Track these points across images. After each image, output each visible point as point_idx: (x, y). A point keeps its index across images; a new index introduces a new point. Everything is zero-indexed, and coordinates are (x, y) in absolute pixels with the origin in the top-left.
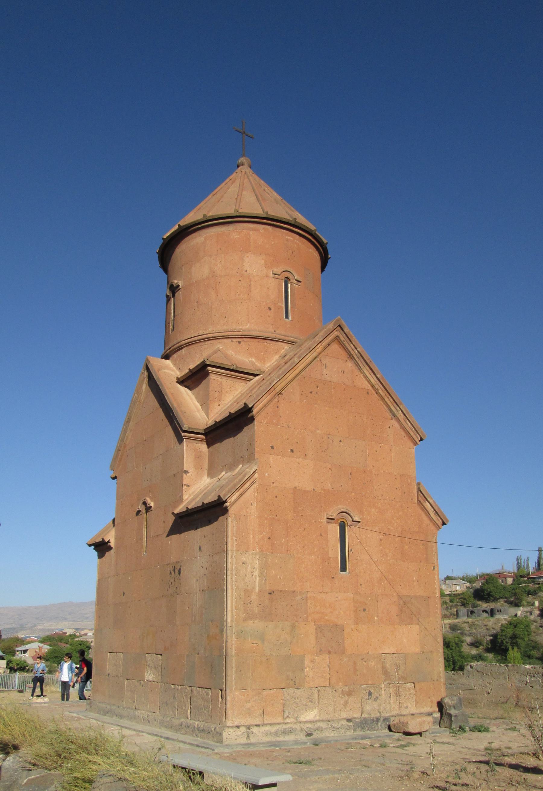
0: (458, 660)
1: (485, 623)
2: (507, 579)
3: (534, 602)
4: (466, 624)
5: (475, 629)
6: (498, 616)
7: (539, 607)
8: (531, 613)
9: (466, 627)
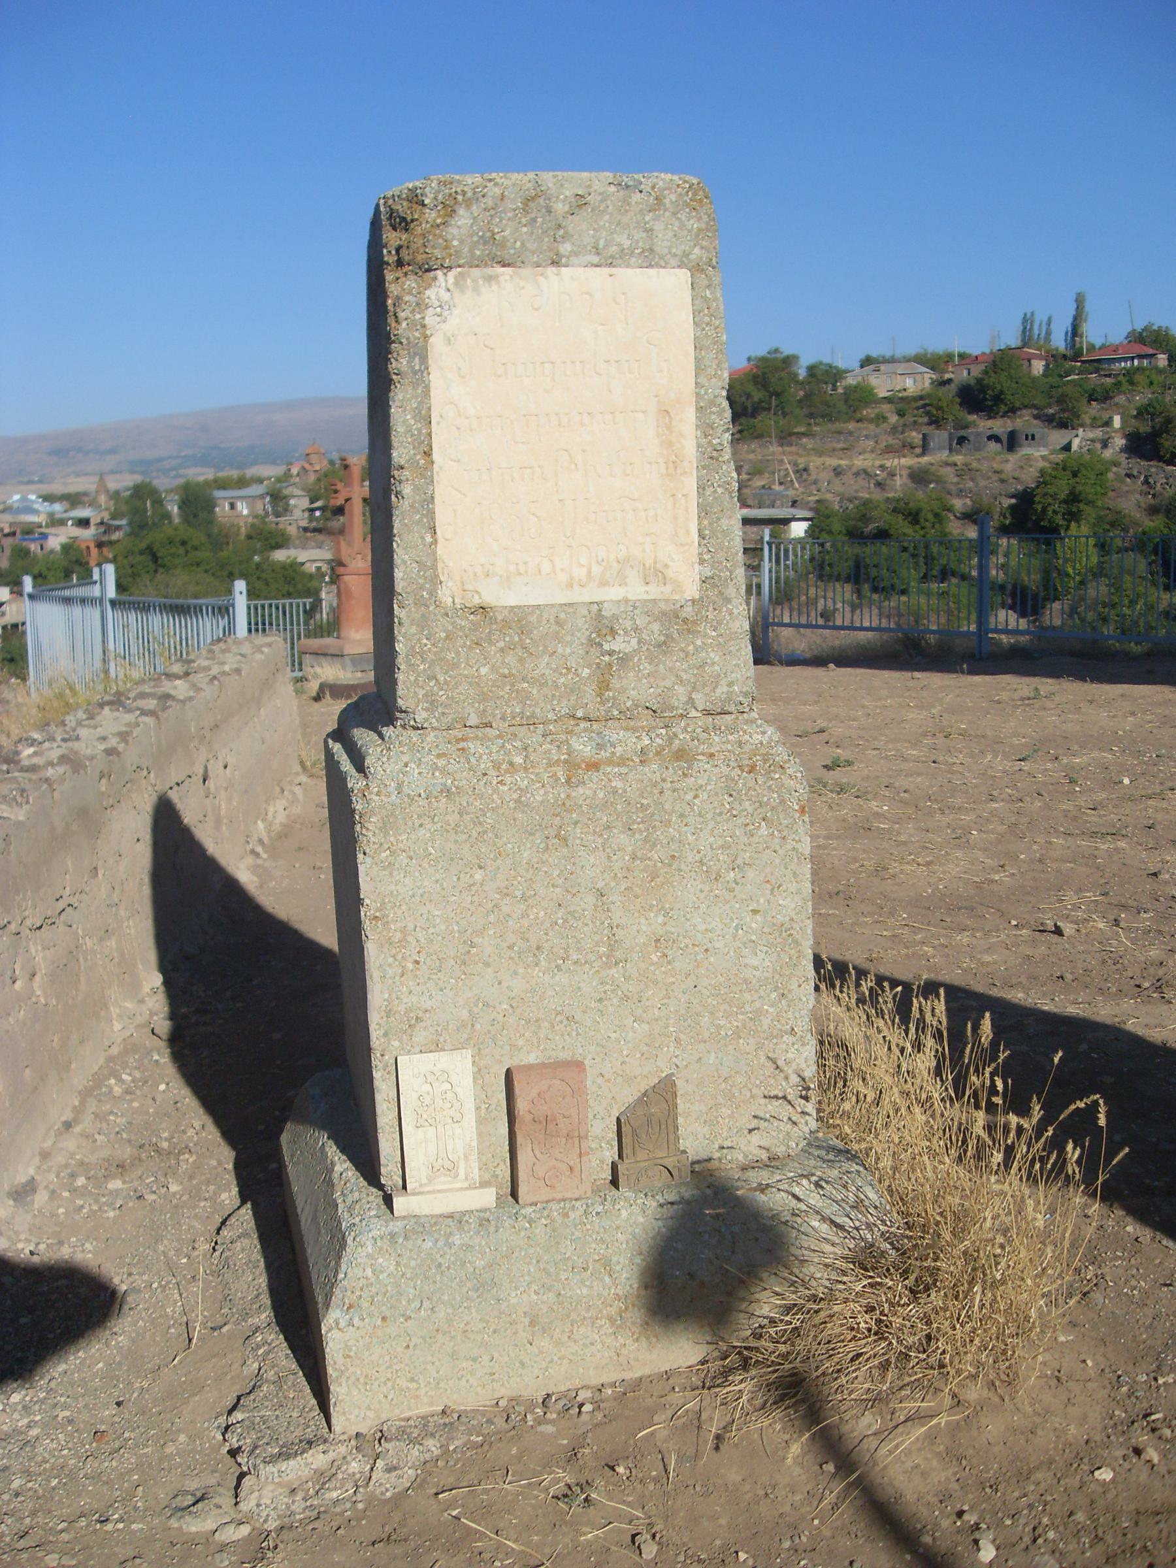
0: (940, 554)
1: (996, 466)
2: (1033, 362)
3: (1111, 418)
4: (949, 469)
5: (972, 480)
6: (1026, 450)
7: (1122, 428)
8: (1105, 444)
9: (949, 474)
